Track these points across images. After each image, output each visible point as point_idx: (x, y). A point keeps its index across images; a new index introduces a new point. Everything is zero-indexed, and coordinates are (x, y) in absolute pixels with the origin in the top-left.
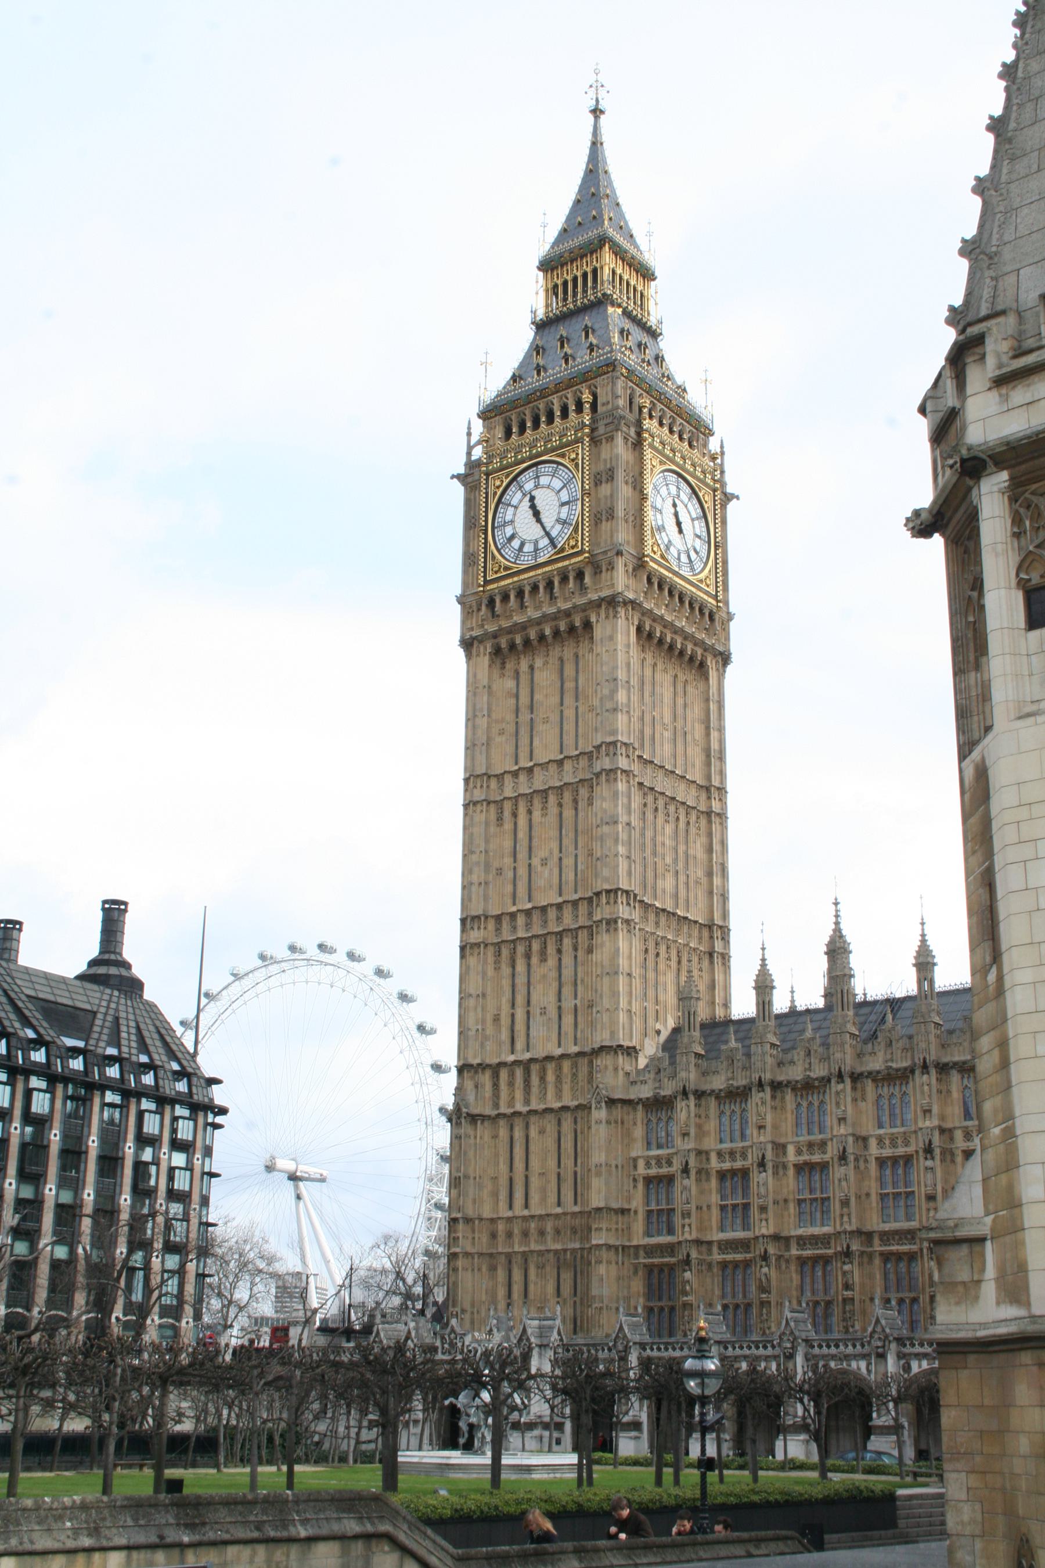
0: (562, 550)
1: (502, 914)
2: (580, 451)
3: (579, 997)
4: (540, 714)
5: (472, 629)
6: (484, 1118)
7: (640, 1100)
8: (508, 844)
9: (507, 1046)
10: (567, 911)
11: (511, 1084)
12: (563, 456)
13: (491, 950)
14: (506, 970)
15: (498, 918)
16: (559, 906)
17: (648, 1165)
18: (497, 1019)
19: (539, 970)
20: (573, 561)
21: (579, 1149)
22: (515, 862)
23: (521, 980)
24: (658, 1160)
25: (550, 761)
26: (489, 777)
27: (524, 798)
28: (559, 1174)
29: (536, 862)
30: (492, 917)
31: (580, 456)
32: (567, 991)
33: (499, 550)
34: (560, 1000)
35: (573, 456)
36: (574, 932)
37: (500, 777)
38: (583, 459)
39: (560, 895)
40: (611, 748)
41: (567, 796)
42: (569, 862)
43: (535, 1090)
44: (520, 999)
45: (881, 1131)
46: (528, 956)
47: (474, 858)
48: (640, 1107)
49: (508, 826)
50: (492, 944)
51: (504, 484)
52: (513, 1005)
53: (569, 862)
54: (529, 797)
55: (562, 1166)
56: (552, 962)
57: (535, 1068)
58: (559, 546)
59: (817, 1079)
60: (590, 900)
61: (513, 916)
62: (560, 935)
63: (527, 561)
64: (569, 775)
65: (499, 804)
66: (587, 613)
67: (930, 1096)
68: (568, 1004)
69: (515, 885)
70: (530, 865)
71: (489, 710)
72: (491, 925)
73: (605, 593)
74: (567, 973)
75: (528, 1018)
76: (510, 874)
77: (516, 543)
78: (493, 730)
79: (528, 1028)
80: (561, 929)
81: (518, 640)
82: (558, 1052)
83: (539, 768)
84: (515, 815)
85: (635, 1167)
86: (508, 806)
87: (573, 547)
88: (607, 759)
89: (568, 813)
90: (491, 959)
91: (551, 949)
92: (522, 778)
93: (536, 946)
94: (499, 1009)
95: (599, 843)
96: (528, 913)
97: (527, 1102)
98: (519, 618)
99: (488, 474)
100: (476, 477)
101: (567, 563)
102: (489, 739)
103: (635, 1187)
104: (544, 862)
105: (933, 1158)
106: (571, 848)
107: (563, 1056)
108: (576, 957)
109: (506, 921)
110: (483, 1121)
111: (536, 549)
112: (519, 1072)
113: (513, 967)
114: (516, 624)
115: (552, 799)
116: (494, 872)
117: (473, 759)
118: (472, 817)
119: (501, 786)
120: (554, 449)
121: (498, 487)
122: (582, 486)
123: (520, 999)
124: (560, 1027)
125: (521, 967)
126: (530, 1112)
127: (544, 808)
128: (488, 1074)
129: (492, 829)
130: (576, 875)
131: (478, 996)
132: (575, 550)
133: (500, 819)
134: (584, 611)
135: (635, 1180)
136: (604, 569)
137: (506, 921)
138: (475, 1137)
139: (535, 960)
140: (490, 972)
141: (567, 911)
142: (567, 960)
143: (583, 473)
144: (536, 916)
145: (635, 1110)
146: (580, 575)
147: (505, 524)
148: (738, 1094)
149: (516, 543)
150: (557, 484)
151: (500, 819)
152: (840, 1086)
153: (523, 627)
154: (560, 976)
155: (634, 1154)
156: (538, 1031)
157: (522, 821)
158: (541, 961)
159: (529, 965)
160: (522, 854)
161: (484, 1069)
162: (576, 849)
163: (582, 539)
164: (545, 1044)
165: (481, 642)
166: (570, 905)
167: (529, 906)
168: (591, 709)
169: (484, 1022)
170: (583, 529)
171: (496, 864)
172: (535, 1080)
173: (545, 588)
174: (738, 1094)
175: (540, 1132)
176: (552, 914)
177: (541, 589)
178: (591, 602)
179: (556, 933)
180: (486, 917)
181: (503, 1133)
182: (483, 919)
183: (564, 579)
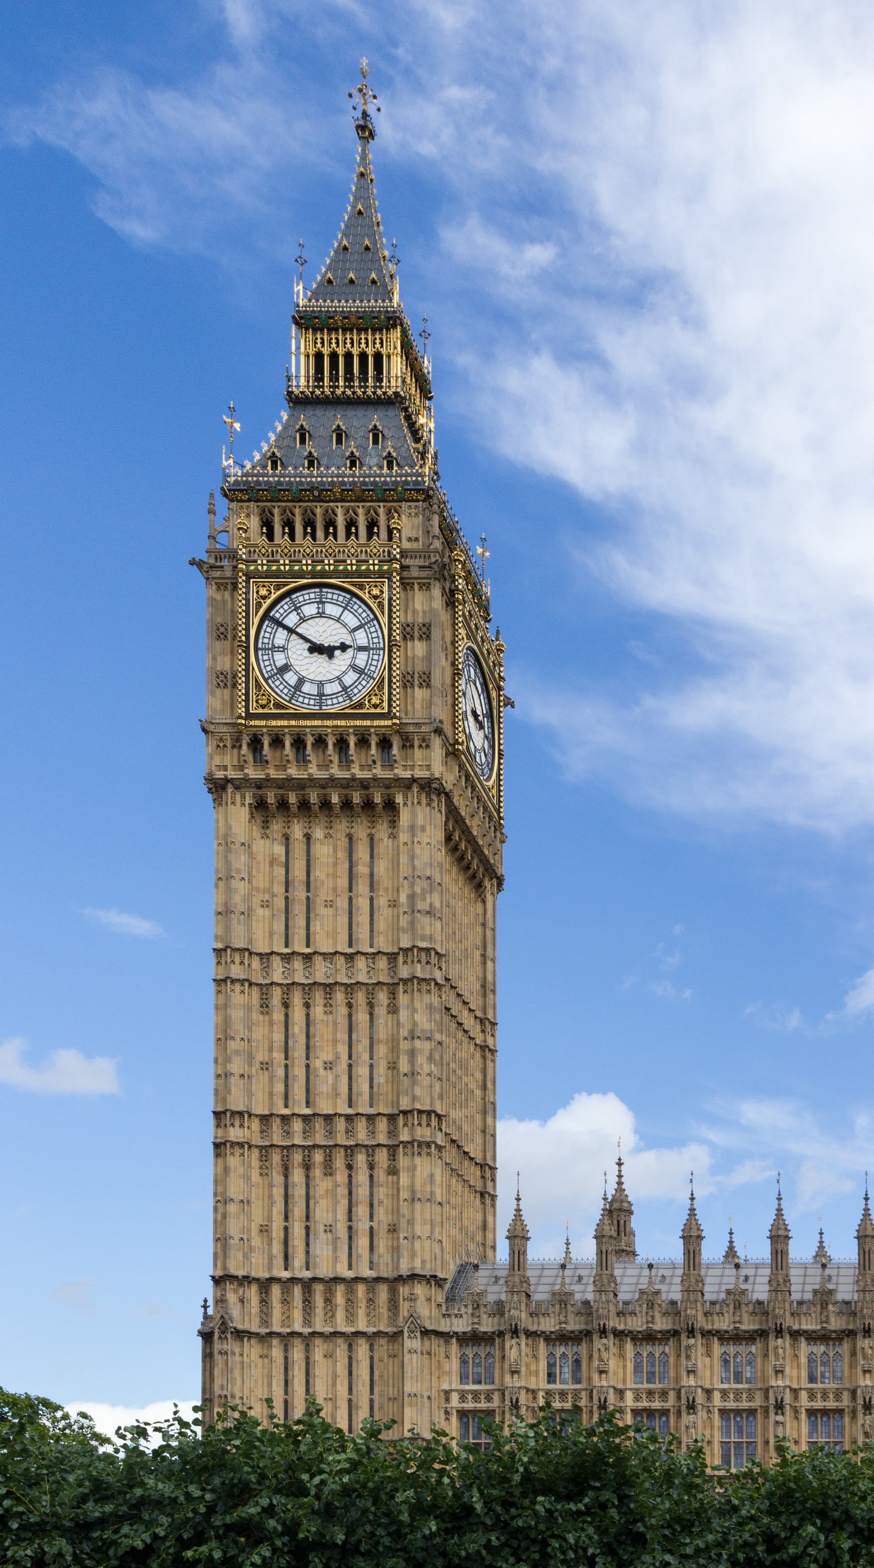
0: (360, 705)
1: (271, 1115)
2: (386, 589)
3: (375, 1218)
4: (323, 894)
5: (225, 768)
6: (250, 1334)
7: (456, 1333)
8: (278, 1036)
9: (279, 1261)
10: (361, 1126)
11: (285, 1302)
12: (361, 587)
13: (256, 1153)
14: (278, 1179)
15: (265, 1119)
16: (349, 1118)
17: (463, 1398)
18: (264, 1230)
19: (322, 1185)
20: (376, 723)
21: (376, 1377)
22: (286, 1058)
23: (299, 1192)
24: (476, 1395)
25: (336, 953)
26: (251, 954)
27: (300, 988)
28: (350, 1401)
29: (318, 1064)
30: (257, 1116)
31: (386, 595)
32: (362, 1211)
33: (266, 680)
34: (350, 1220)
35: (376, 592)
36: (370, 1150)
37: (265, 957)
38: (390, 599)
39: (350, 1106)
40: (423, 955)
41: (361, 997)
42: (362, 1071)
43: (319, 1311)
44: (298, 1211)
45: (726, 1386)
46: (307, 1167)
47: (233, 1045)
48: (454, 1340)
49: (278, 1016)
50: (257, 1147)
51: (273, 597)
52: (286, 1218)
53: (362, 1071)
54: (309, 988)
55: (354, 1392)
56: (341, 1176)
57: (319, 1288)
58: (356, 699)
59: (660, 1332)
60: (392, 1118)
61: (285, 1119)
62: (350, 1151)
63: (306, 705)
64: (362, 972)
65: (265, 989)
66: (392, 791)
67: (784, 1358)
68: (363, 1225)
69: (286, 1086)
70: (308, 1066)
71: (250, 874)
72: (256, 1125)
73: (419, 773)
74: (362, 1192)
75: (308, 1235)
76: (281, 1072)
77: (291, 678)
78: (254, 899)
79: (308, 1245)
80: (352, 1143)
81: (293, 799)
82: (350, 1274)
83: (320, 958)
84: (286, 1005)
85: (447, 1400)
86: (277, 993)
87: (375, 706)
88: (419, 966)
89: (362, 1016)
90: (255, 1163)
91: (339, 1162)
92: (298, 964)
93: (318, 1157)
94: (270, 1218)
95: (406, 1057)
96: (306, 1118)
97: (307, 1322)
98: (293, 772)
99: (249, 576)
100: (228, 574)
101: (368, 723)
102: (250, 909)
103: (447, 1419)
104: (329, 1066)
105: (783, 1414)
106: (366, 1056)
107: (357, 1280)
108: (371, 1176)
109: (276, 1123)
110: (249, 1338)
111: (321, 695)
112: (297, 1291)
113: (286, 1177)
114: (290, 779)
115: (340, 996)
116: (258, 1065)
117: (228, 928)
118: (227, 998)
119: (266, 969)
120: (346, 574)
121: (264, 598)
122: (390, 635)
123: (298, 1211)
124: (350, 1248)
125: (297, 1176)
126: (313, 1334)
127: (328, 1004)
128: (254, 1288)
129: (255, 1016)
130: (371, 1087)
131: (242, 1201)
132: (378, 711)
133: (265, 1006)
134: (388, 787)
135: (447, 1412)
136: (416, 743)
137: (276, 1123)
138: (242, 1355)
139: (317, 1172)
140: (255, 1177)
141: (361, 1126)
142: (362, 1177)
143: (390, 617)
144: (319, 1125)
145: (447, 1342)
146: (385, 744)
147: (274, 649)
148: (570, 1338)
149: (291, 678)
150: (351, 620)
151: (265, 1006)
152: (692, 1341)
153: (301, 785)
154: (350, 1193)
155: (446, 1387)
156: (322, 1248)
157: (298, 1014)
158: (325, 1174)
159: (307, 1177)
160: (298, 1052)
161: (250, 1282)
162: (371, 1058)
163: (390, 699)
164: (328, 1261)
165: (237, 788)
166: (364, 1119)
167: (308, 1111)
168: (394, 904)
169: (249, 1230)
170: (390, 687)
171: (261, 1056)
172: (319, 1300)
173: (334, 745)
174: (570, 1338)
175: (325, 1356)
176: (341, 1125)
177: (330, 746)
178: (398, 780)
179: (346, 1147)
180: (250, 1115)
181: (277, 1352)
182: (246, 1116)
183: (363, 742)
